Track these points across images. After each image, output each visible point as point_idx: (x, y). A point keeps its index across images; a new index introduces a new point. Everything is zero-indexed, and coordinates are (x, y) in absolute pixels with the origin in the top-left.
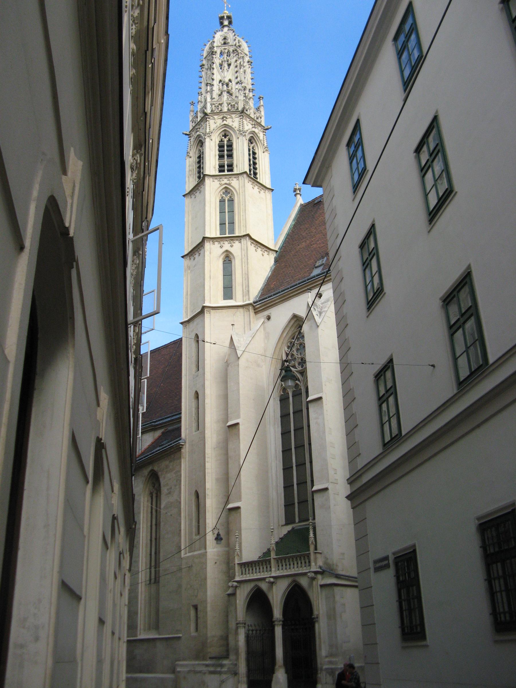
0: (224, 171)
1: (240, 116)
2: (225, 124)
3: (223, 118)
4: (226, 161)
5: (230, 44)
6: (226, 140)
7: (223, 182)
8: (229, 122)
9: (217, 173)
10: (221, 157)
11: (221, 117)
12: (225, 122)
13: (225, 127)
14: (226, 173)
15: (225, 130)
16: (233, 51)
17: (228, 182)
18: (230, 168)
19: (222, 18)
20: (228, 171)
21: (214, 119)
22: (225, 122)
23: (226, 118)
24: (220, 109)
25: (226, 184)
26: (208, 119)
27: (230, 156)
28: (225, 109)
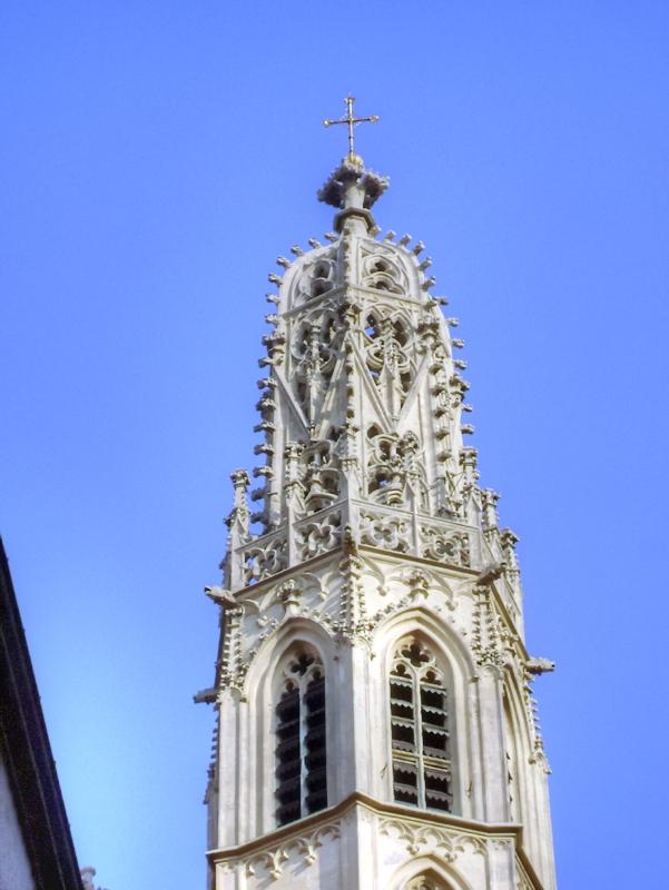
0: (413, 799)
1: (477, 593)
2: (421, 609)
3: (412, 583)
4: (421, 760)
5: (406, 297)
6: (418, 673)
7: (424, 849)
8: (434, 600)
9: (392, 803)
10: (402, 735)
11: (408, 574)
12: (420, 600)
13: (419, 620)
14: (422, 808)
15: (417, 634)
16: (421, 329)
17: (441, 853)
18: (435, 794)
19: (348, 176)
20: (431, 803)
21: (377, 573)
22: (420, 600)
23: (426, 585)
24: (395, 543)
25: (431, 857)
26: (353, 568)
27: (436, 742)
28: (295, 559)
